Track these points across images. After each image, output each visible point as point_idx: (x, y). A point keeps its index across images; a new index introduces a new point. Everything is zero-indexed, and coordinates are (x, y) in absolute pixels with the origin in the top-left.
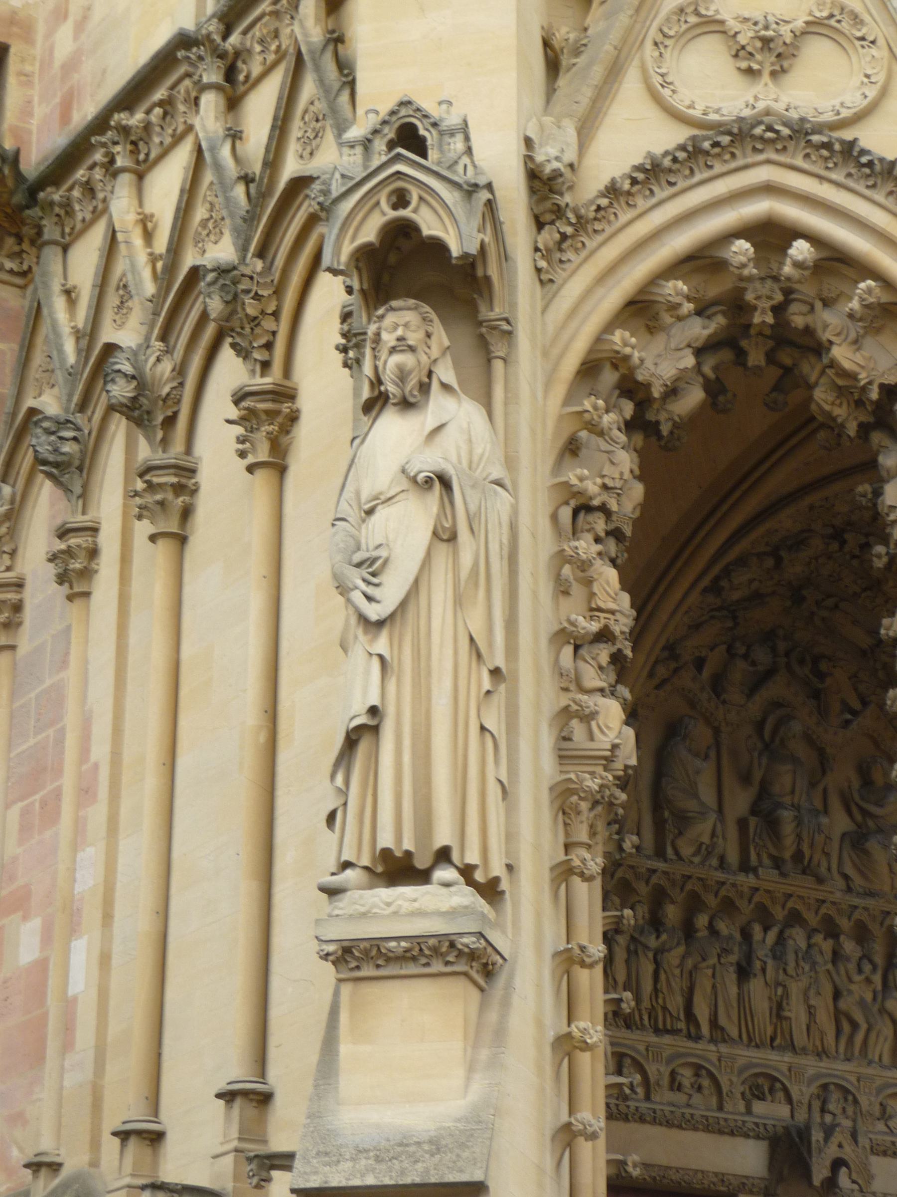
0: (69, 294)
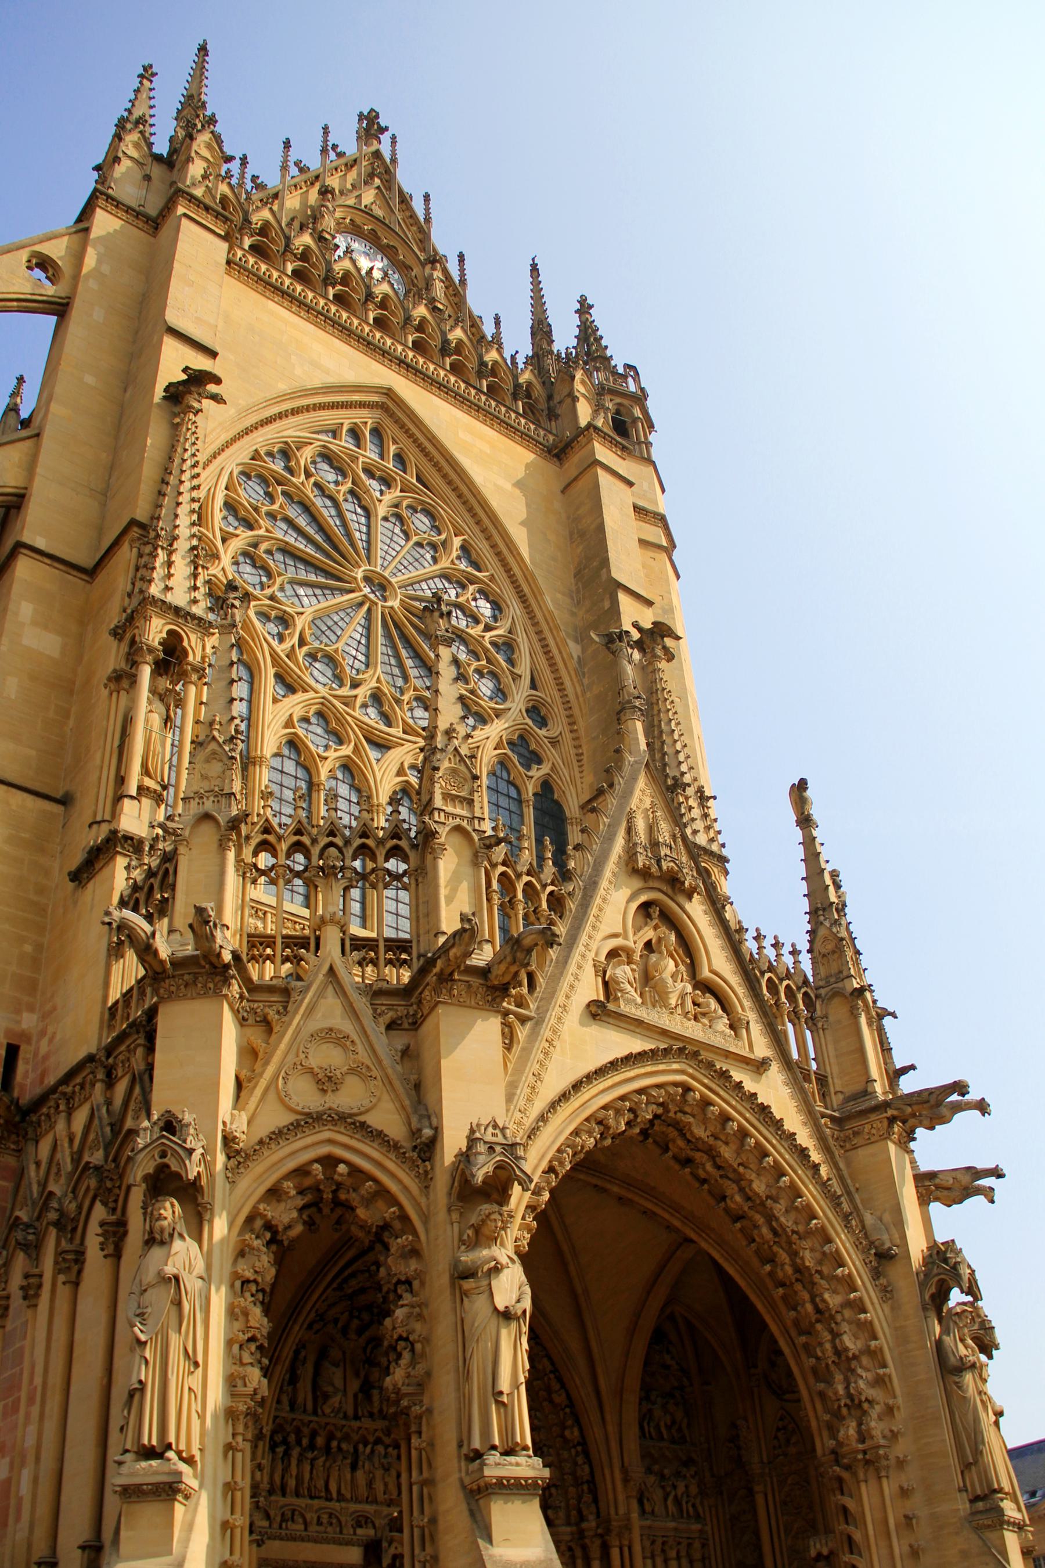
0: (38, 1164)
